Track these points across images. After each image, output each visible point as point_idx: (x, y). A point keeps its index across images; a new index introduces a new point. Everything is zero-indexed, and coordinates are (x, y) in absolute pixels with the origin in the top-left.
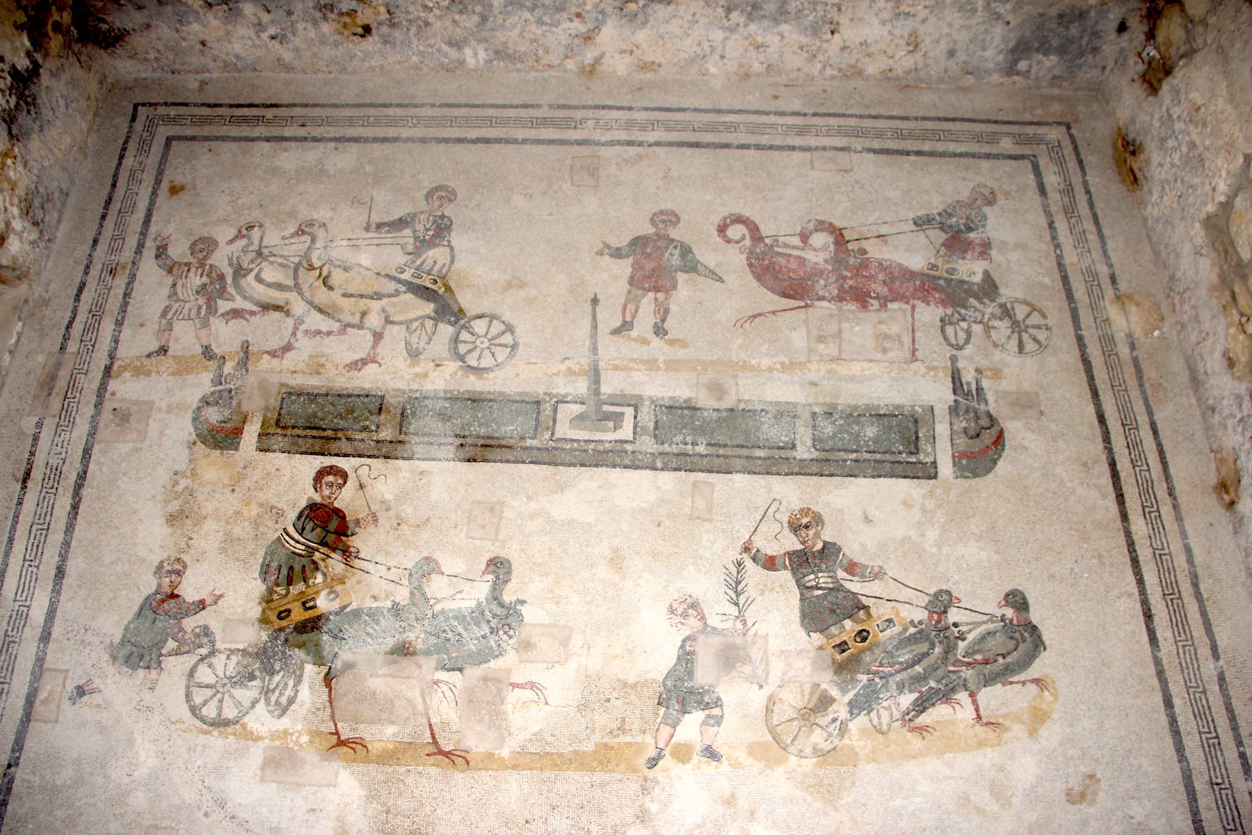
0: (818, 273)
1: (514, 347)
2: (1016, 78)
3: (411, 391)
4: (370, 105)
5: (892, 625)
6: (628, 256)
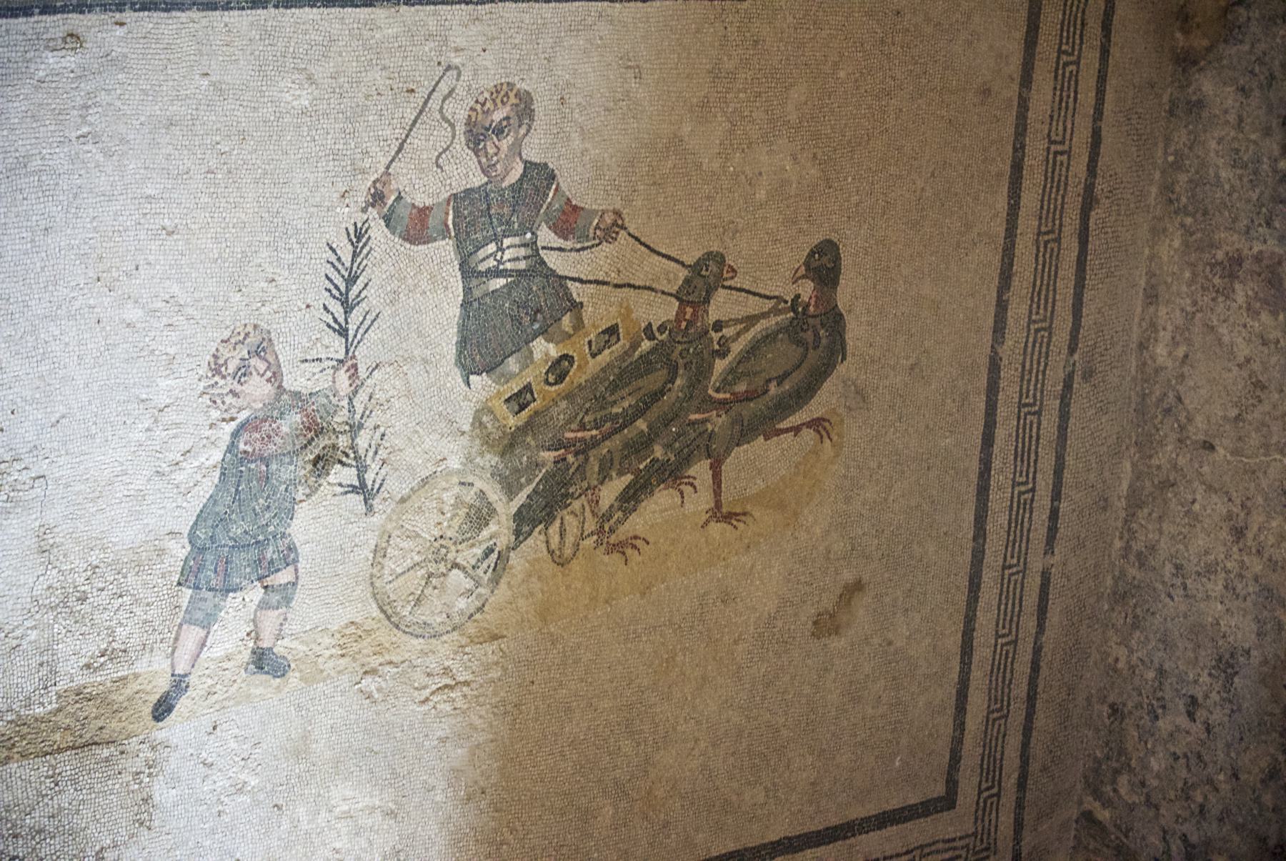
5: (614, 339)
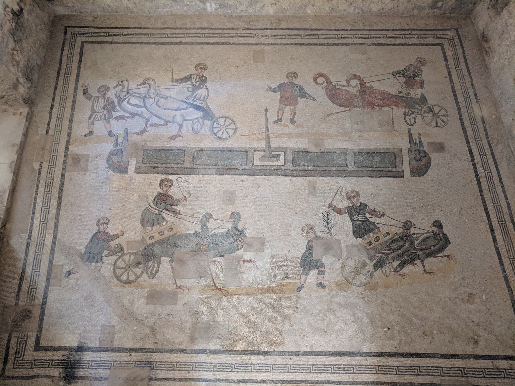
0: (353, 96)
1: (236, 129)
2: (435, 10)
3: (196, 147)
4: (167, 28)
6: (278, 91)
